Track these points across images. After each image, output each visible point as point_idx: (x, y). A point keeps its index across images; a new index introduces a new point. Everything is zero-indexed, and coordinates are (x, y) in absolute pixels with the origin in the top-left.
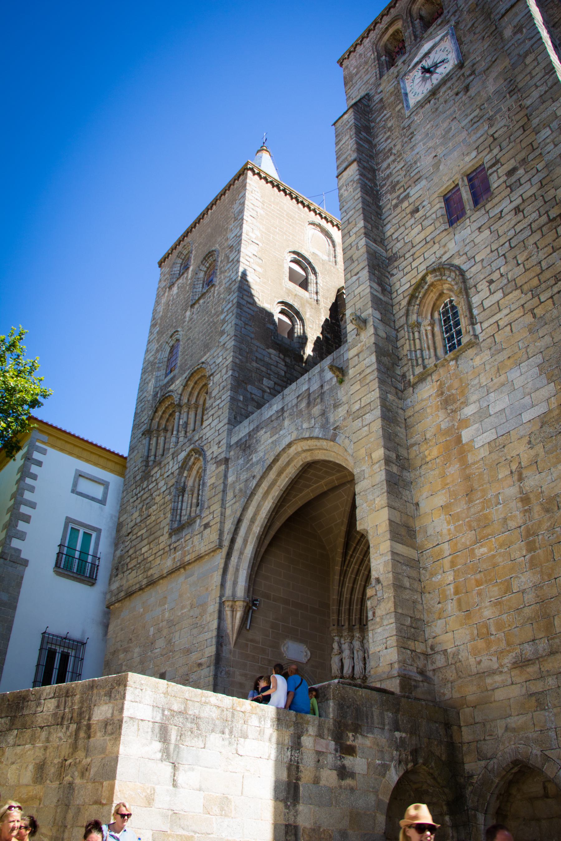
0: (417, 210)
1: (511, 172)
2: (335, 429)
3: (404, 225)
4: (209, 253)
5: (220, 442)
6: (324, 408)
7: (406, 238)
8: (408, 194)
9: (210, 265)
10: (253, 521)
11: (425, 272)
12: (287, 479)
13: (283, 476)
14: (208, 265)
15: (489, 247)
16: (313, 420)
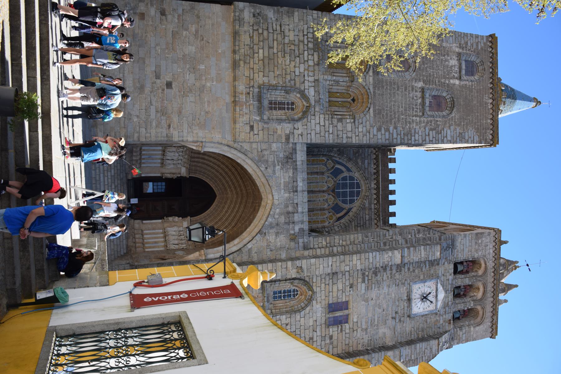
0: (350, 288)
1: (331, 337)
2: (265, 234)
3: (349, 279)
4: (454, 107)
5: (302, 136)
6: (281, 225)
7: (341, 280)
8: (364, 282)
9: (447, 102)
10: (244, 161)
11: (315, 291)
12: (259, 185)
13: (262, 185)
14: (448, 100)
15: (303, 324)
16: (277, 217)
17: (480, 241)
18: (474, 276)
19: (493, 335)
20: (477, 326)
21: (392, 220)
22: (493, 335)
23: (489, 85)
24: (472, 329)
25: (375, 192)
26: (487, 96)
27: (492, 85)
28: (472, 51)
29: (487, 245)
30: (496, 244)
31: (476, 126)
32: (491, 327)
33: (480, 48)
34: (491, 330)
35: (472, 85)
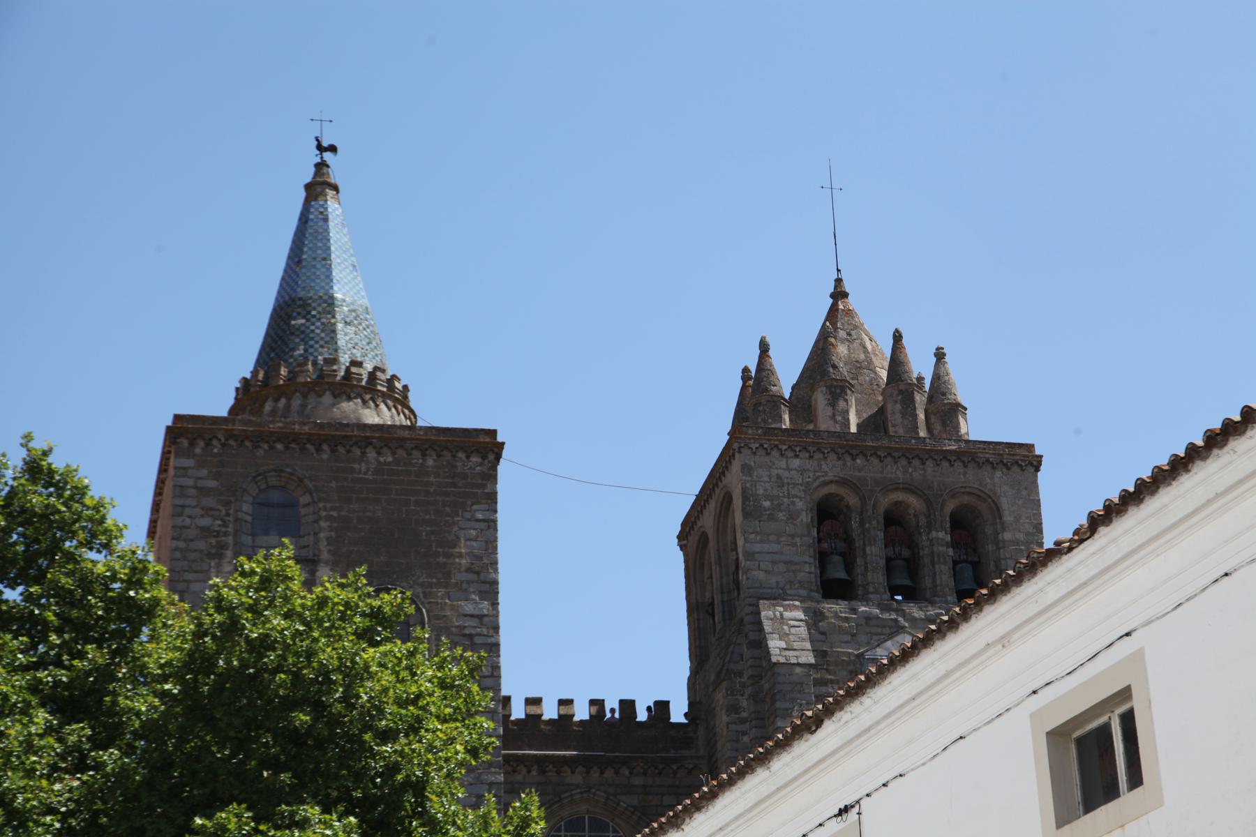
17: (767, 504)
18: (862, 524)
19: (1031, 464)
20: (1000, 518)
21: (678, 714)
22: (1031, 464)
23: (325, 456)
24: (1007, 536)
25: (595, 774)
26: (357, 466)
27: (325, 447)
28: (228, 515)
29: (779, 477)
30: (776, 446)
31: (448, 509)
32: (1008, 469)
33: (213, 484)
34: (1016, 469)
35: (329, 518)
